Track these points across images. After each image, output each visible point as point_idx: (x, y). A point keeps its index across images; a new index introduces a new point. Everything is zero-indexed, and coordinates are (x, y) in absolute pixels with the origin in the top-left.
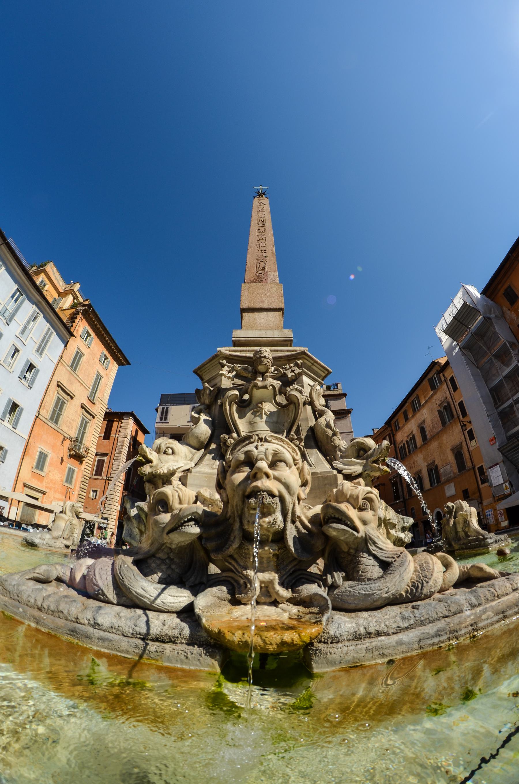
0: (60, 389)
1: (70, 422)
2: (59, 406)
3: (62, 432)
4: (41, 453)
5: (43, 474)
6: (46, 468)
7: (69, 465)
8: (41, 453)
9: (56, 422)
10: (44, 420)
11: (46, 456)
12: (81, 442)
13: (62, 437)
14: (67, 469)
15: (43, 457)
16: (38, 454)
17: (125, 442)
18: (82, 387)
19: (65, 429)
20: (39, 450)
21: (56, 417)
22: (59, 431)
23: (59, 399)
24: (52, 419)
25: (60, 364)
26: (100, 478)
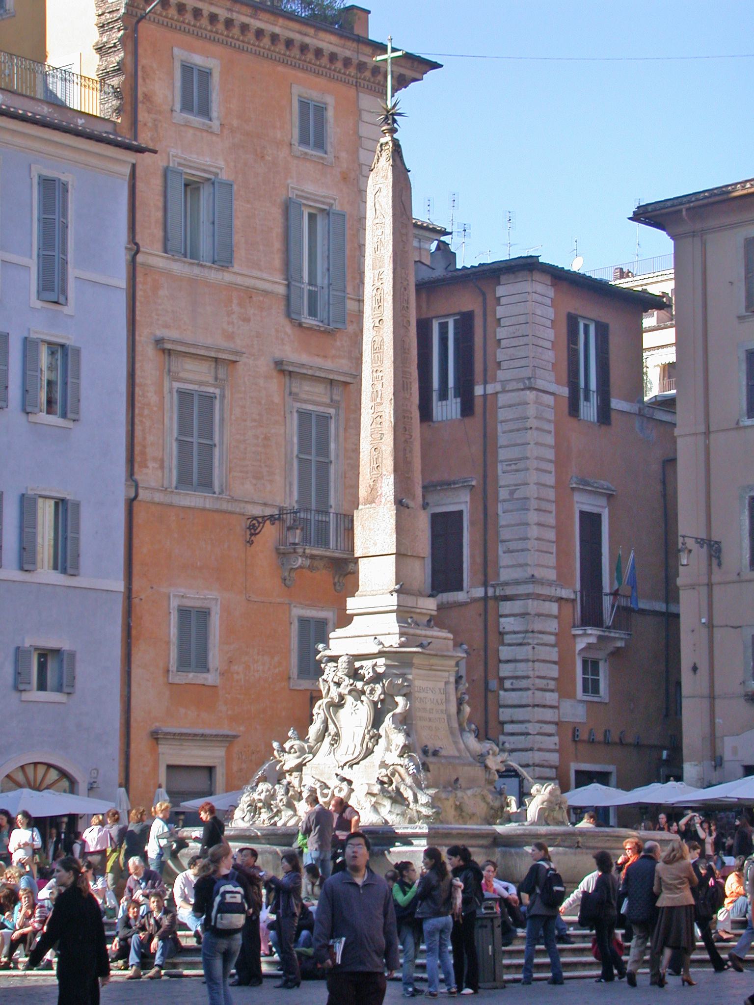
2: (196, 411)
4: (184, 613)
5: (210, 678)
6: (215, 658)
7: (298, 611)
8: (184, 613)
9: (206, 483)
10: (158, 497)
11: (204, 614)
12: (324, 511)
14: (295, 626)
15: (194, 620)
16: (174, 618)
17: (531, 411)
19: (244, 488)
20: (174, 603)
21: (195, 470)
22: (225, 506)
23: (185, 397)
24: (184, 480)
26: (461, 596)
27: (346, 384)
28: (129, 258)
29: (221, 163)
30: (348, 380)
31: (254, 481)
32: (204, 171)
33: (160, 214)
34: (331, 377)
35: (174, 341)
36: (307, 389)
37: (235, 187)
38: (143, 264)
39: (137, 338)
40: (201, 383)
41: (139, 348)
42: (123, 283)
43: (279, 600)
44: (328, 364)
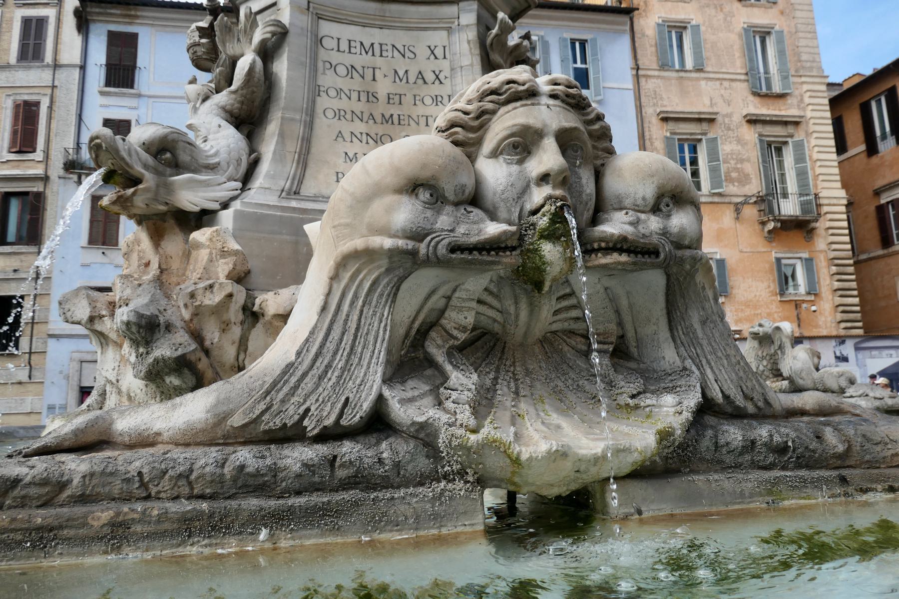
0: (671, 126)
1: (736, 170)
3: (727, 200)
13: (732, 207)
18: (726, 84)
25: (643, 81)
27: (797, 124)
28: (634, 72)
29: (692, 17)
30: (798, 120)
31: (736, 184)
32: (681, 22)
33: (653, 49)
34: (785, 119)
35: (667, 112)
36: (769, 130)
37: (702, 28)
38: (644, 76)
39: (644, 114)
40: (691, 134)
41: (646, 121)
42: (631, 87)
43: (763, 250)
44: (783, 113)
